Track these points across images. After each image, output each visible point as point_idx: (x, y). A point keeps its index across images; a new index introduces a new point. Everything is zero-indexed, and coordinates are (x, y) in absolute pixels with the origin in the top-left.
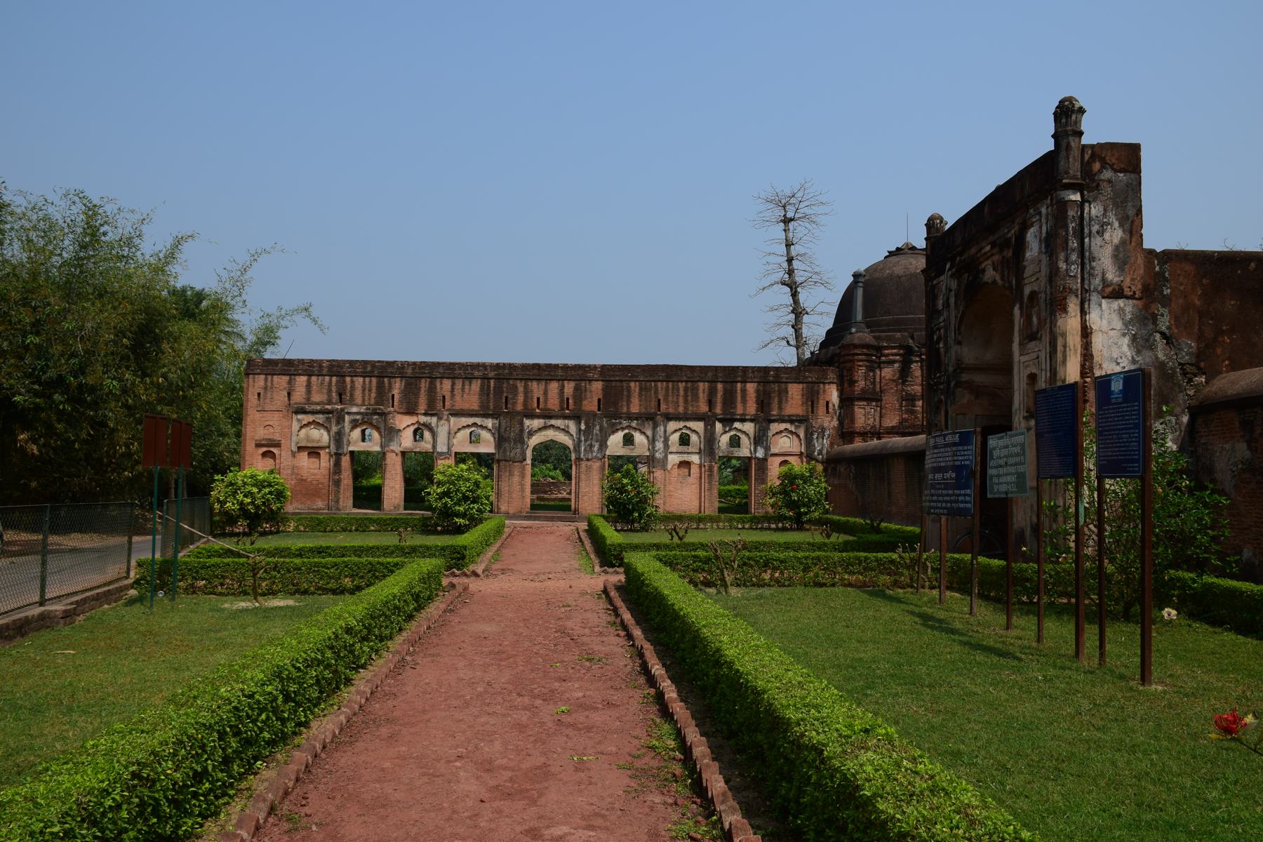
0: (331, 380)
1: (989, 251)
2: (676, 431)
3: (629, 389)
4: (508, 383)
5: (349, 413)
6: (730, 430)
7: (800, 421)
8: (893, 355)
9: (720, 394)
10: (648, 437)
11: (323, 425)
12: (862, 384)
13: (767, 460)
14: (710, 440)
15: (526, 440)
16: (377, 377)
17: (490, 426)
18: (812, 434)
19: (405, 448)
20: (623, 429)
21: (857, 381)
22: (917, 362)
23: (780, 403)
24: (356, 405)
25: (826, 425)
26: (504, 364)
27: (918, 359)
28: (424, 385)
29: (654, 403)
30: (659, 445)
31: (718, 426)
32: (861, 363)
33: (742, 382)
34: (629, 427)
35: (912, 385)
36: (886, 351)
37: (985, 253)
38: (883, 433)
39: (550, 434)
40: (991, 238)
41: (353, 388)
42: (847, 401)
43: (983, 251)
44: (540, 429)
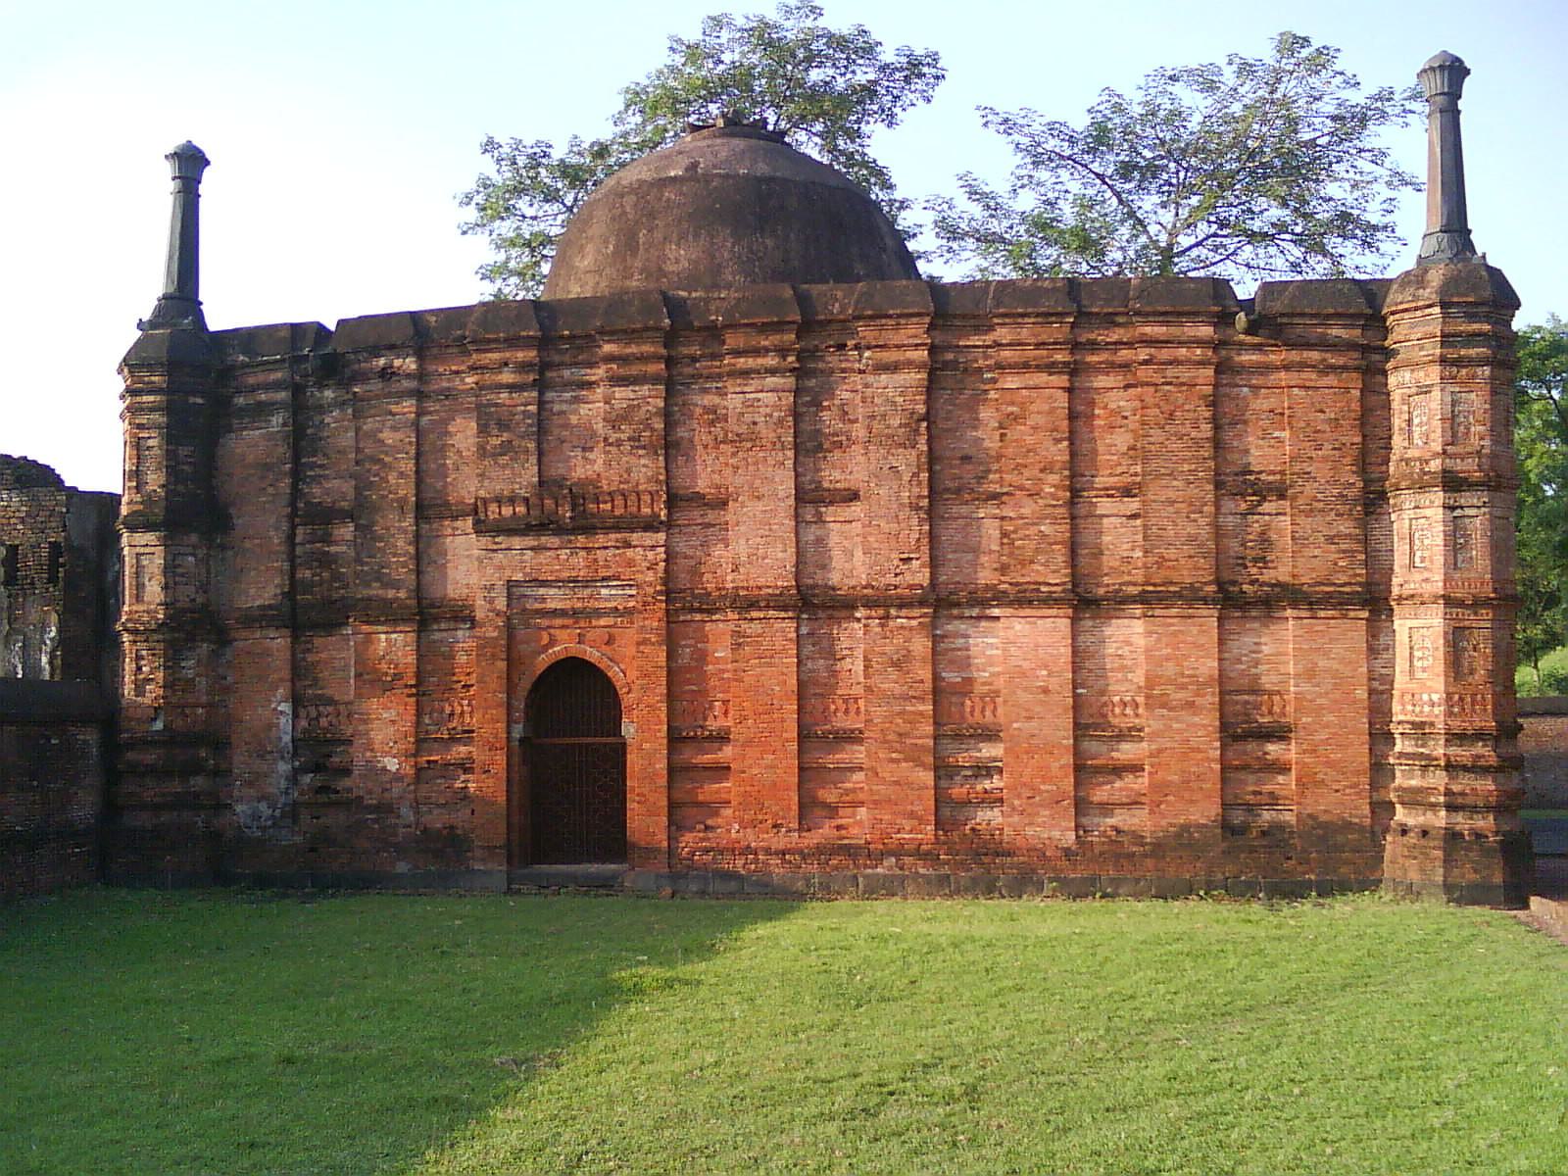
8: (268, 387)
35: (325, 477)
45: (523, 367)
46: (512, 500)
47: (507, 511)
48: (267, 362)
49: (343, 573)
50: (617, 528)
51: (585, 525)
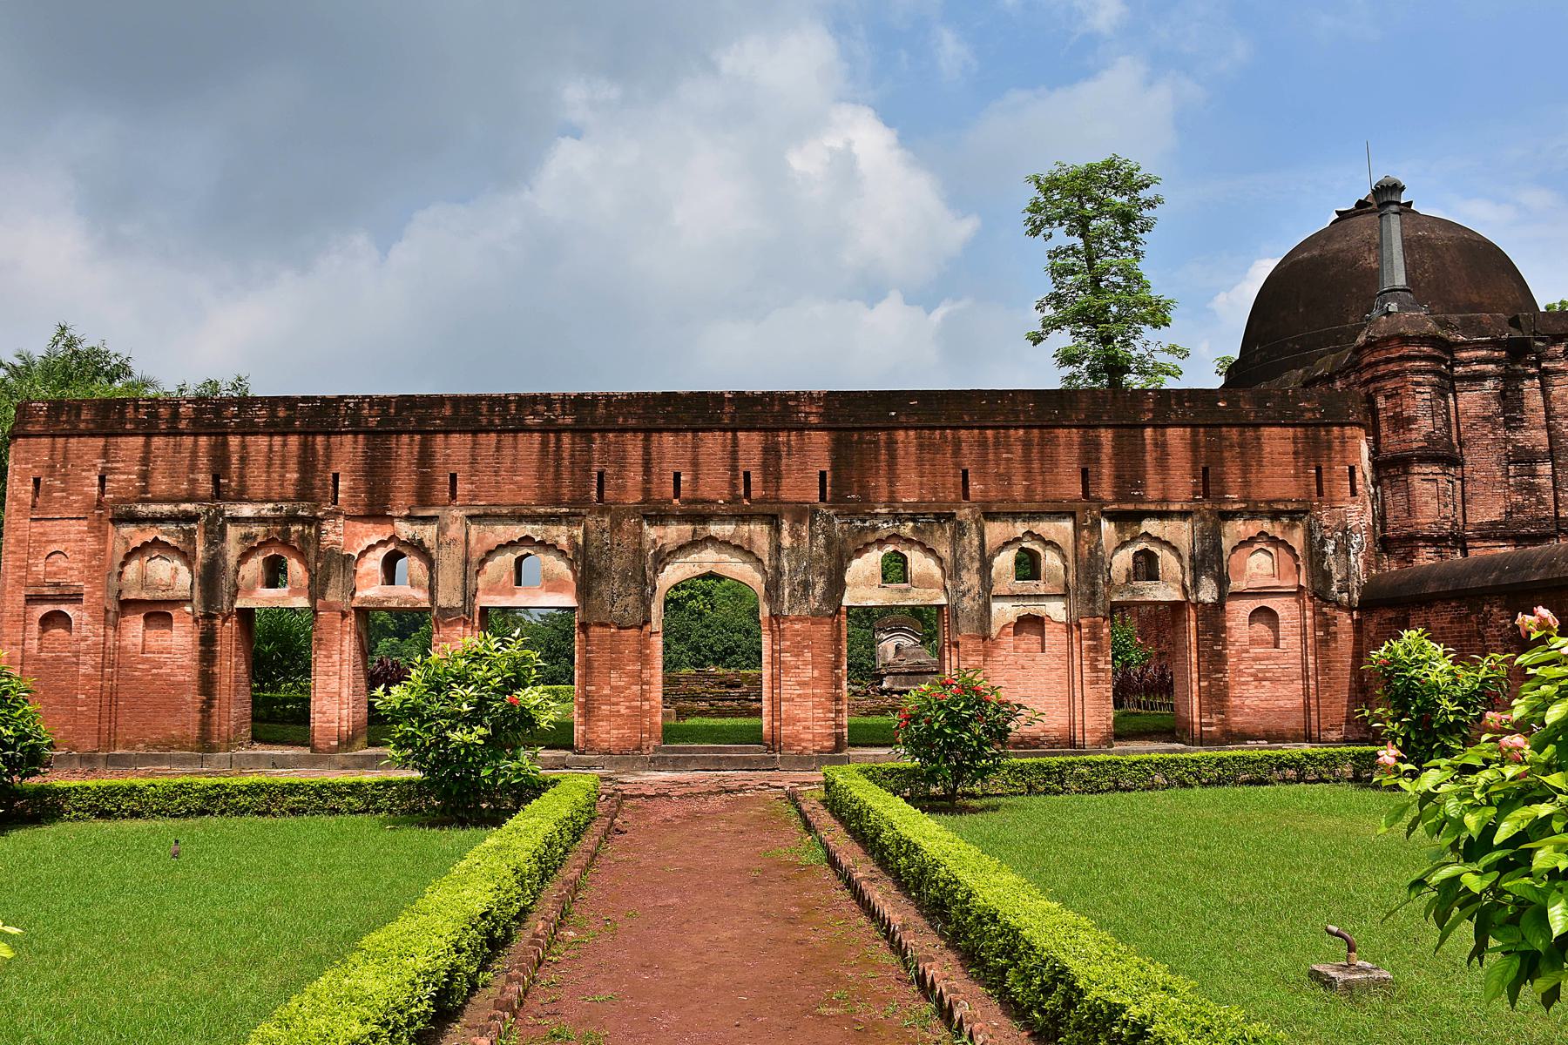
0: (196, 443)
2: (1007, 544)
3: (891, 443)
4: (603, 438)
5: (235, 520)
6: (1133, 539)
7: (1294, 516)
8: (1480, 361)
10: (940, 560)
11: (176, 548)
12: (1425, 425)
13: (1223, 607)
14: (1090, 567)
15: (650, 573)
16: (299, 433)
17: (563, 541)
18: (1323, 543)
19: (364, 600)
20: (881, 543)
22: (1531, 377)
23: (1245, 472)
24: (250, 501)
25: (1353, 522)
26: (594, 396)
27: (1533, 370)
28: (405, 448)
29: (953, 480)
30: (971, 579)
31: (1107, 527)
32: (1419, 378)
33: (1155, 427)
34: (895, 537)
35: (1526, 429)
36: (1464, 355)
38: (1473, 540)
42: (1389, 468)
44: (682, 548)
48: (1478, 342)
49: (1545, 499)
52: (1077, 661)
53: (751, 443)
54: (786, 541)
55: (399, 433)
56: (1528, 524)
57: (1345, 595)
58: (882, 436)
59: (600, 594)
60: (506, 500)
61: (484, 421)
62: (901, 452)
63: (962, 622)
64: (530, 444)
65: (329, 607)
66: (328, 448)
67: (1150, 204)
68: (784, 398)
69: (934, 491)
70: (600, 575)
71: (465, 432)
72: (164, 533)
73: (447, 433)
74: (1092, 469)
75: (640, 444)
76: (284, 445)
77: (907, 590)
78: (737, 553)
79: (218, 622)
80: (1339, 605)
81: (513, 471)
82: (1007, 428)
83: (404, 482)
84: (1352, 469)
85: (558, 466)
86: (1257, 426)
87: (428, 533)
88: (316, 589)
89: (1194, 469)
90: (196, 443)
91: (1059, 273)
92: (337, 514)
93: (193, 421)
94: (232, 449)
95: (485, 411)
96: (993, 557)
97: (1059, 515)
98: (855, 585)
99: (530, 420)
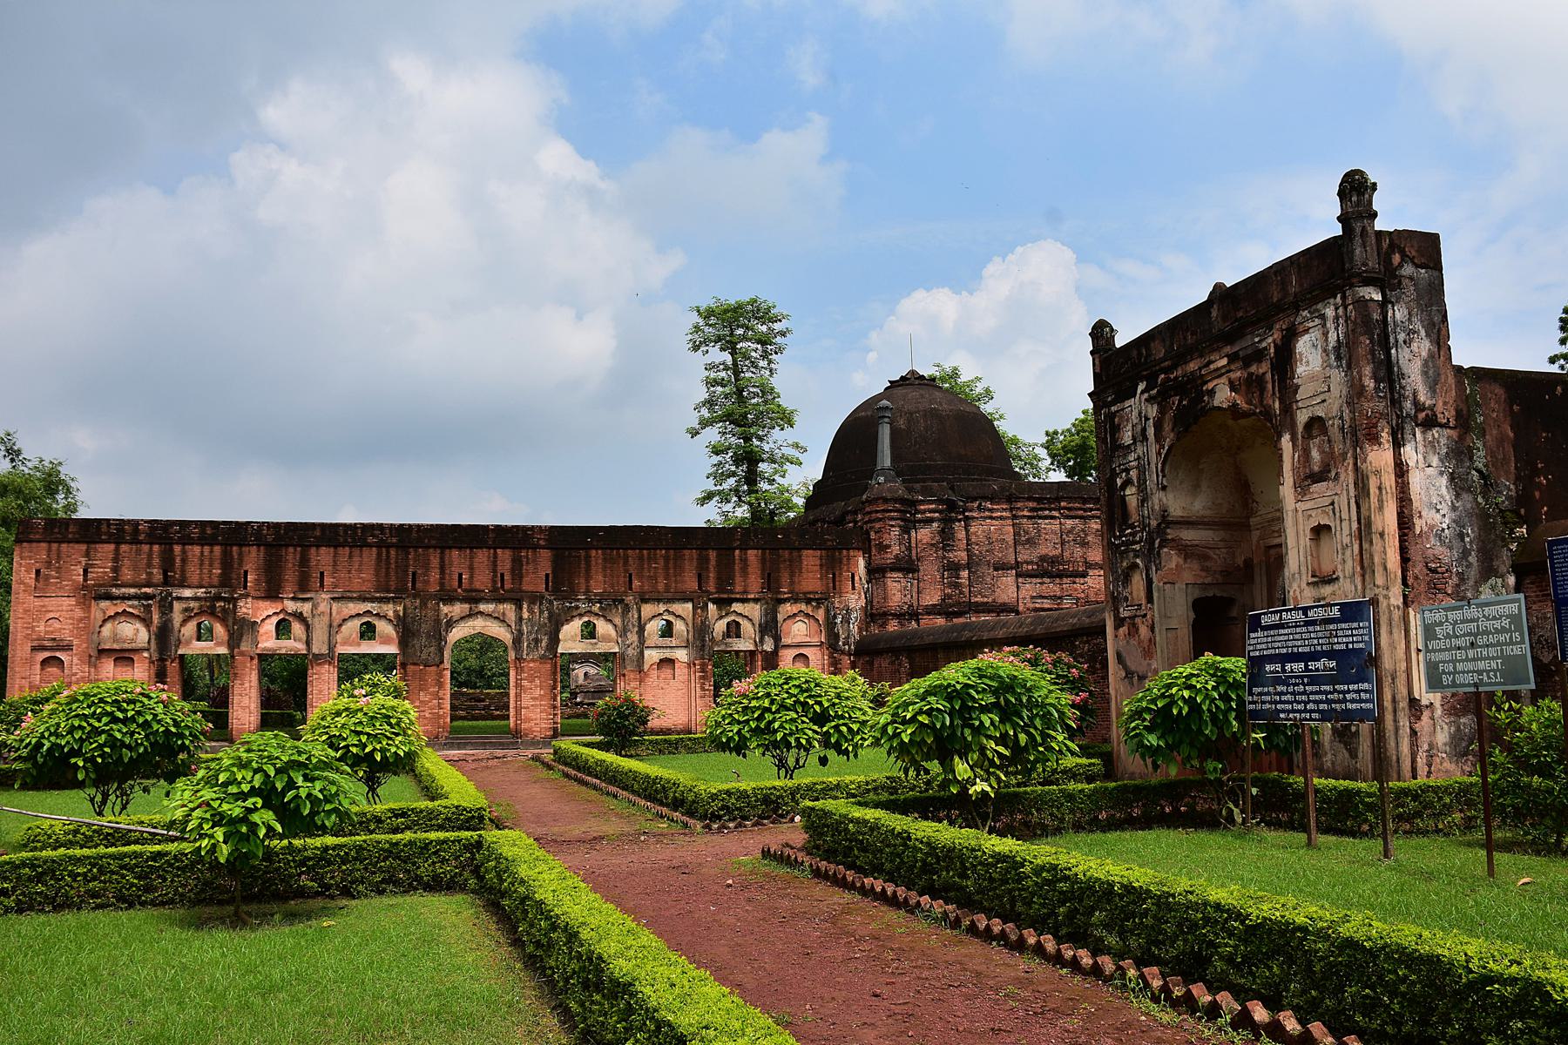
0: (151, 549)
1: (1224, 366)
3: (588, 557)
4: (416, 551)
5: (179, 599)
6: (727, 614)
8: (931, 511)
9: (713, 562)
11: (138, 617)
12: (896, 549)
13: (777, 655)
16: (221, 545)
18: (835, 617)
19: (264, 649)
20: (581, 615)
21: (889, 546)
22: (960, 521)
23: (792, 575)
24: (189, 587)
25: (852, 606)
28: (291, 556)
30: (633, 638)
33: (741, 549)
37: (1218, 369)
38: (922, 615)
39: (478, 625)
40: (1228, 349)
41: (184, 561)
42: (876, 573)
43: (1212, 367)
45: (1032, 510)
46: (1031, 563)
47: (1030, 567)
50: (1070, 576)
51: (1060, 575)
52: (693, 685)
53: (505, 556)
54: (525, 615)
55: (287, 546)
56: (954, 605)
57: (847, 647)
58: (582, 553)
59: (413, 646)
60: (356, 588)
61: (342, 540)
62: (593, 563)
63: (627, 662)
64: (370, 555)
65: (242, 654)
66: (240, 554)
67: (783, 334)
68: (524, 529)
69: (612, 586)
70: (413, 634)
71: (329, 546)
72: (130, 606)
73: (318, 547)
74: (704, 574)
75: (438, 556)
76: (211, 552)
77: (596, 644)
78: (496, 621)
79: (168, 663)
80: (843, 652)
81: (360, 571)
82: (655, 549)
83: (290, 576)
84: (853, 575)
85: (387, 569)
86: (799, 549)
87: (306, 608)
88: (234, 641)
89: (763, 574)
90: (151, 549)
91: (712, 383)
92: (246, 596)
93: (148, 535)
94: (176, 553)
95: (341, 533)
96: (645, 624)
97: (685, 600)
98: (565, 640)
99: (370, 539)
